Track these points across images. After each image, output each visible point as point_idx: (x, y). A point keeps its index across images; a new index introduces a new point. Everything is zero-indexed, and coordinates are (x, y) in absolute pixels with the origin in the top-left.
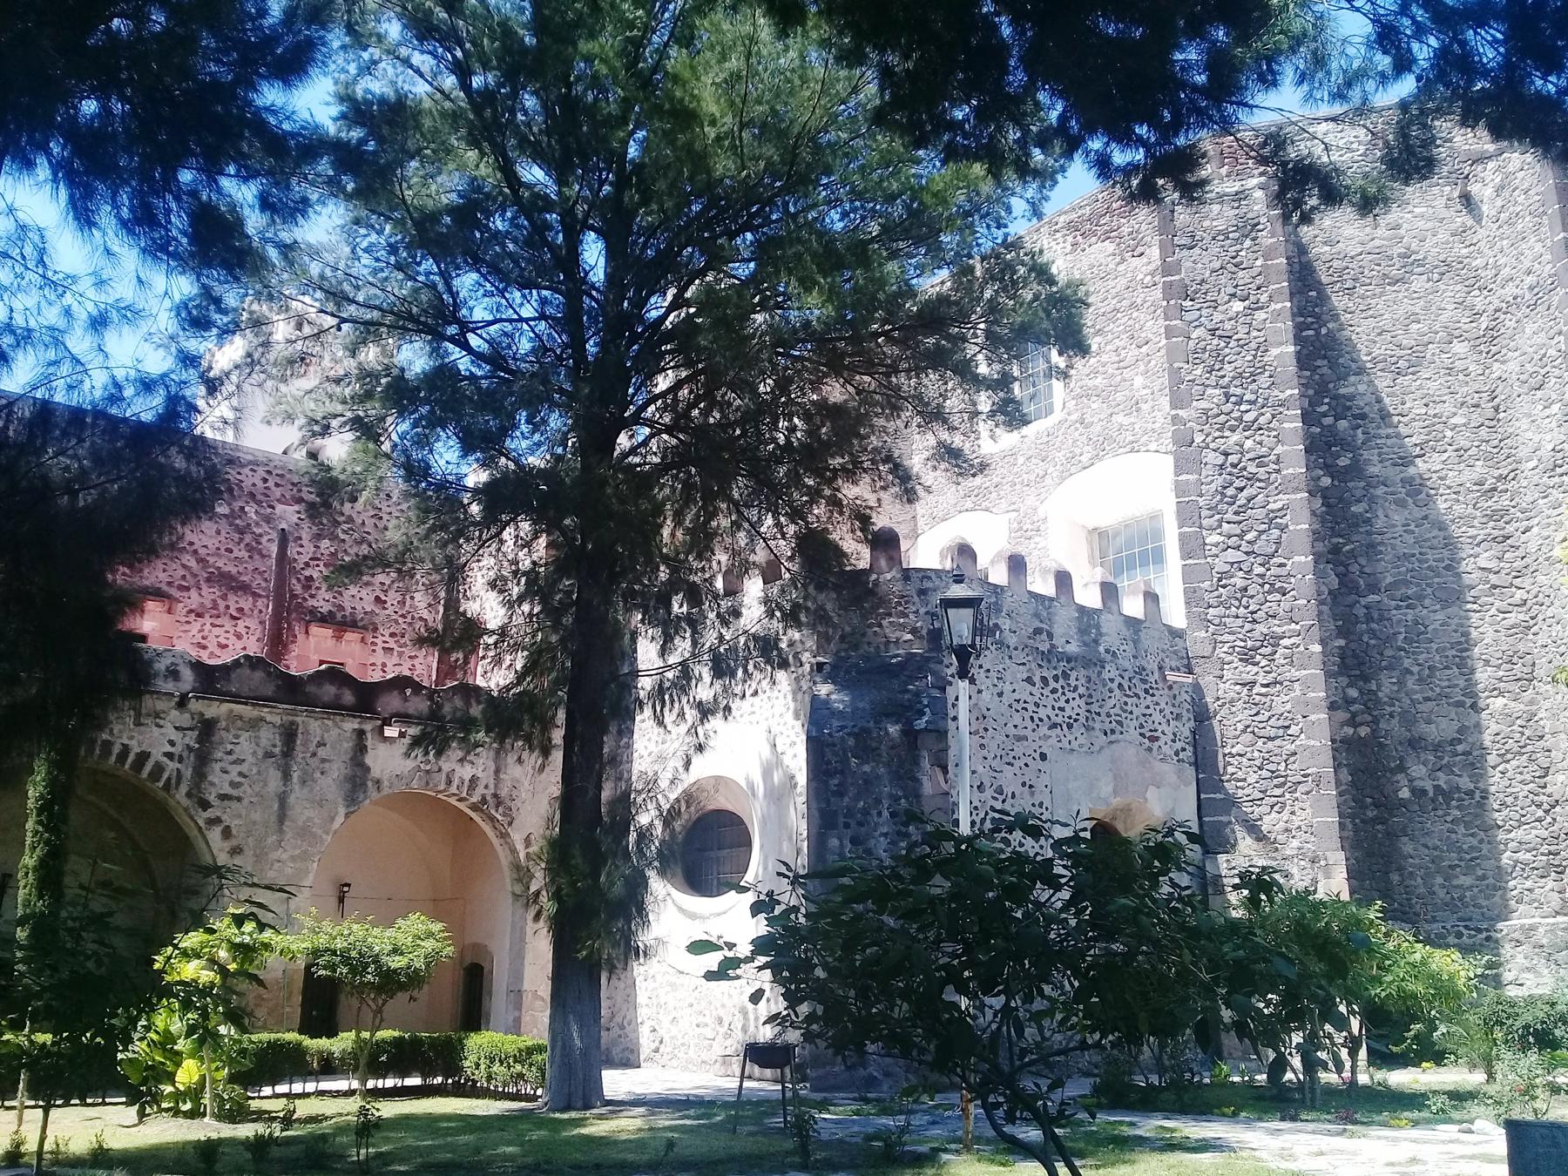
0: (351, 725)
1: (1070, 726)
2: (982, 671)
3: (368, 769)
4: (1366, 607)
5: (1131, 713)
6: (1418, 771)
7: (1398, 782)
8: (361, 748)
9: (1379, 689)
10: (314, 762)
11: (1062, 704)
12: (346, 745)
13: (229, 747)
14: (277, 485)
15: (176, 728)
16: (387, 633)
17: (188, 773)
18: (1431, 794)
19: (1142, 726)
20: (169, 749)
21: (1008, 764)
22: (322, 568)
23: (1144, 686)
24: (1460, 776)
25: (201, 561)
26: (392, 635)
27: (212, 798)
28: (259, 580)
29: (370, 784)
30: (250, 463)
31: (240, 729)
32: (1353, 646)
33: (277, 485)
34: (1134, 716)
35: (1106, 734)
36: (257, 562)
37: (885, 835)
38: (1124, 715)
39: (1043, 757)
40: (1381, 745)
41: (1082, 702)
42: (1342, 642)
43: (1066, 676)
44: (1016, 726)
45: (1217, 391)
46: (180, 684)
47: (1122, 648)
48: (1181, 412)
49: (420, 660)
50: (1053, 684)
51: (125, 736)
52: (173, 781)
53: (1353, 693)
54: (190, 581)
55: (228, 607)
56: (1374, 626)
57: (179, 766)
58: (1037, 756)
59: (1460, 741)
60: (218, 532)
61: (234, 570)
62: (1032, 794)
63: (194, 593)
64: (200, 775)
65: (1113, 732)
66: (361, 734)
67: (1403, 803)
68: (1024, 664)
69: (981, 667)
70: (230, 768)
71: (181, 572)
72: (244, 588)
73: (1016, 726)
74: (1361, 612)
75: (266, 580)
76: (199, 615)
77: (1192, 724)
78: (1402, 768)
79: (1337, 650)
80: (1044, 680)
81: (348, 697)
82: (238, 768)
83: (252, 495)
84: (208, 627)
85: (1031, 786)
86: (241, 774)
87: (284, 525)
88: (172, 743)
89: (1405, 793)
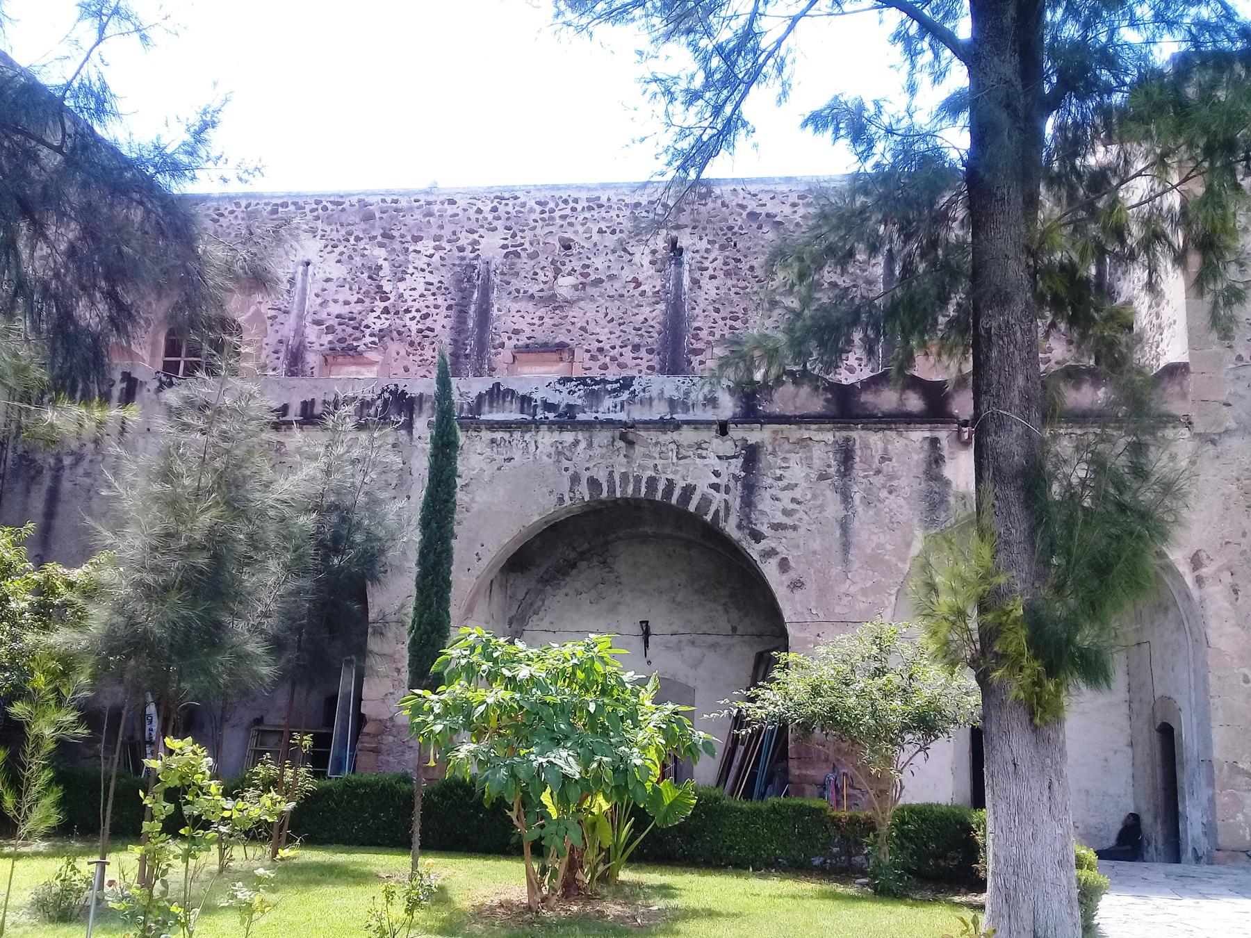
0: (918, 436)
3: (947, 483)
10: (878, 480)
12: (915, 457)
13: (778, 472)
15: (720, 458)
17: (736, 504)
20: (714, 480)
27: (764, 529)
29: (952, 500)
31: (787, 452)
46: (719, 412)
51: (669, 471)
52: (722, 514)
57: (726, 497)
64: (748, 503)
66: (934, 442)
70: (781, 495)
82: (789, 494)
86: (793, 500)
88: (717, 474)
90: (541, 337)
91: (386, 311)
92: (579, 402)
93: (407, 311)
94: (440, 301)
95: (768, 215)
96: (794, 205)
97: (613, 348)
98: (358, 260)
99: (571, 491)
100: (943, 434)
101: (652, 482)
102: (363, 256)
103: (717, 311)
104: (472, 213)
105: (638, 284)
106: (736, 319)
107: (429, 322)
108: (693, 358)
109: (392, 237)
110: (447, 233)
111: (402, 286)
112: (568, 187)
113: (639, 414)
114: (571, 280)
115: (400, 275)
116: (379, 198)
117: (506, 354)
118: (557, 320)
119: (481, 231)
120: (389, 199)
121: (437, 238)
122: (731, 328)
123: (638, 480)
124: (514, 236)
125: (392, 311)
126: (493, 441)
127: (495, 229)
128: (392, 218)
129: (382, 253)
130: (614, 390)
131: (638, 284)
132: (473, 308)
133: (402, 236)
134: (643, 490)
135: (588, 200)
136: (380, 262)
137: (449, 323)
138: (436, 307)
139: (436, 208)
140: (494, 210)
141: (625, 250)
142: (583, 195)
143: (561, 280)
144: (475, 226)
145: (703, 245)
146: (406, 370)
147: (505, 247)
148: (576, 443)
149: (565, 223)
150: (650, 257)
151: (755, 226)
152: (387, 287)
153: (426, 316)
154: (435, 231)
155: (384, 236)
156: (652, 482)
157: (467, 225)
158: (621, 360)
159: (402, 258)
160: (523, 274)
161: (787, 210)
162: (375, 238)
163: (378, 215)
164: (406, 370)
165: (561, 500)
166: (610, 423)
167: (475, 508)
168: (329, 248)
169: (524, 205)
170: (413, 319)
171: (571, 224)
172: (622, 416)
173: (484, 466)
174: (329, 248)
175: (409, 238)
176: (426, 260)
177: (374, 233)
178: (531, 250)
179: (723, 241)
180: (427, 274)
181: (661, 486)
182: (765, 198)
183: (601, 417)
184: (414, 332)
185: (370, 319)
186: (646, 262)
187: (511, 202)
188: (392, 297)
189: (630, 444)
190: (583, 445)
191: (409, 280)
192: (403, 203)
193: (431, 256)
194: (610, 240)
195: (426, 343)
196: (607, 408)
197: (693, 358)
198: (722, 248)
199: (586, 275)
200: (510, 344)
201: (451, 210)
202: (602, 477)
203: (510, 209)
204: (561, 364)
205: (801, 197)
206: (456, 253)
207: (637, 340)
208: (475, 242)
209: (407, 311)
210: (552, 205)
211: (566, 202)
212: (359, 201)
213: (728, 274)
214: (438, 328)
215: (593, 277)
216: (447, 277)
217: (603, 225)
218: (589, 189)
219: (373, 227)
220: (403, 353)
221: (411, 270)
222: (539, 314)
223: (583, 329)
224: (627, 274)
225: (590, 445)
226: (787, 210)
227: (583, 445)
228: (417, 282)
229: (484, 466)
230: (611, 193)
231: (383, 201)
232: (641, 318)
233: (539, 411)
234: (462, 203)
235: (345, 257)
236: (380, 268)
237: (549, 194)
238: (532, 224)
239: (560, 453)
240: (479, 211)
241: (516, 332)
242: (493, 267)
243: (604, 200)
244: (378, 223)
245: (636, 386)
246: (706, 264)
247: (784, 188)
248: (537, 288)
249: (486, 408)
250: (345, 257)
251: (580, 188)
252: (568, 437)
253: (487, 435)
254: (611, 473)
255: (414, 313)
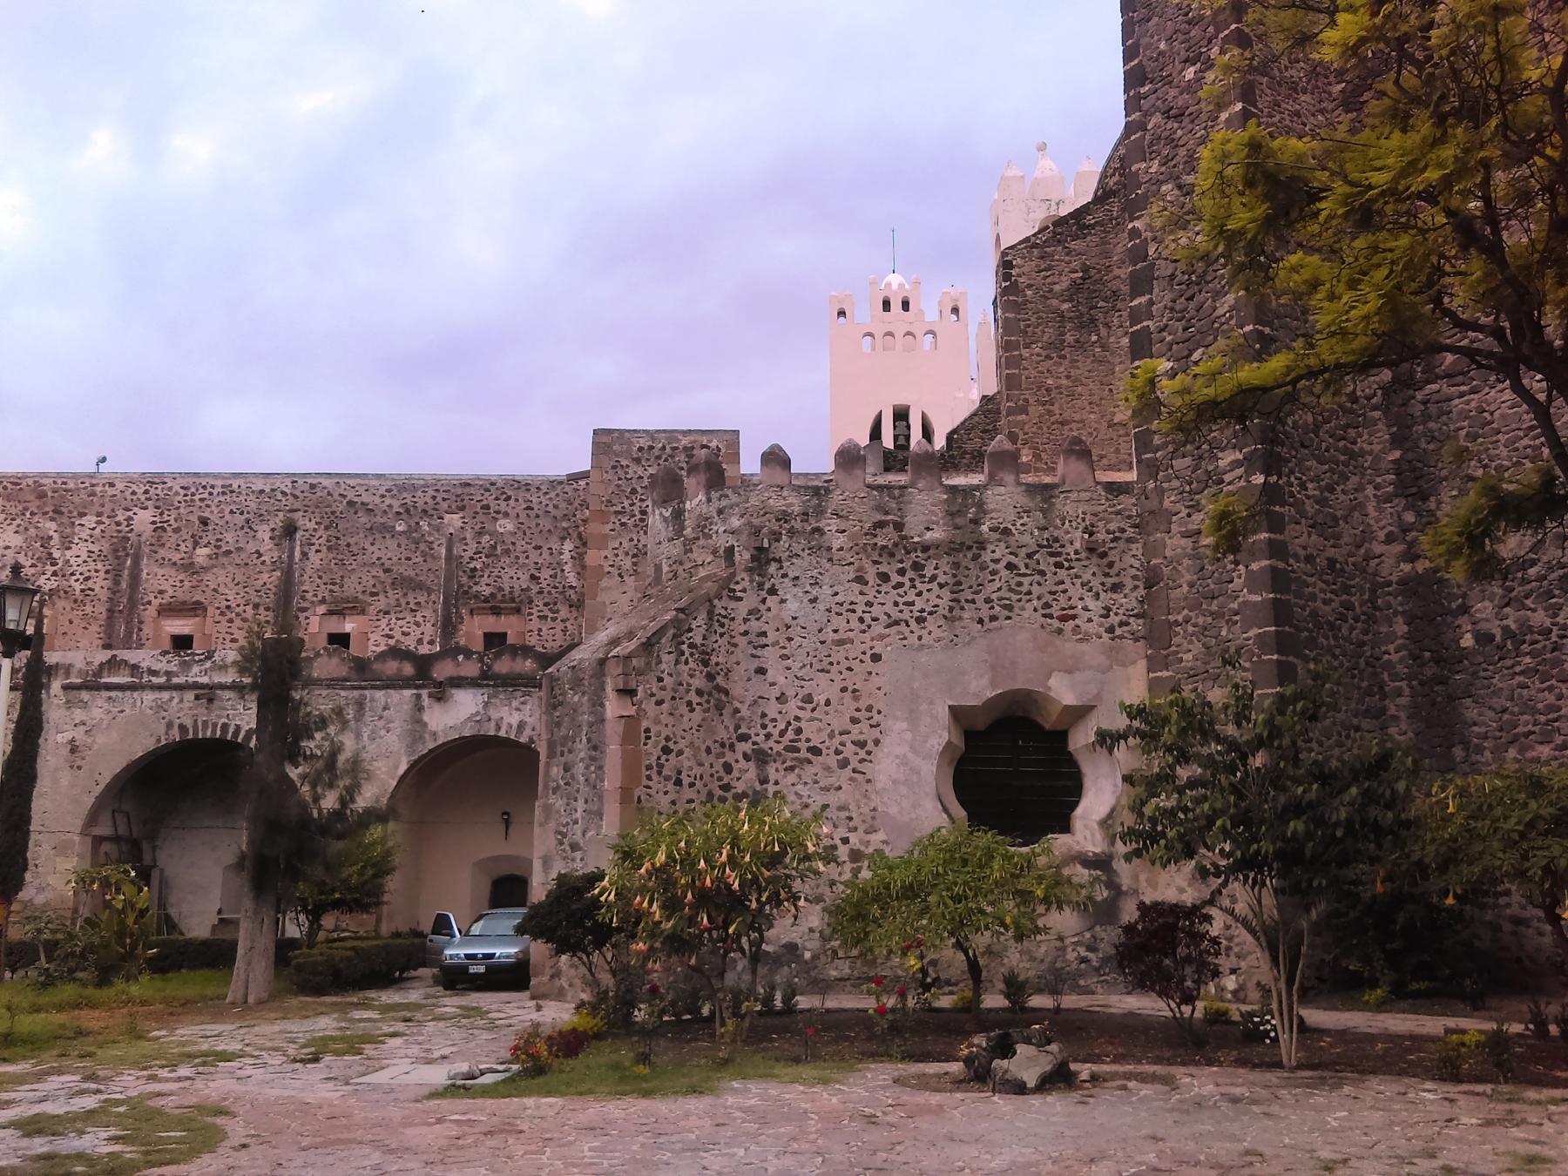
0: (408, 693)
1: (920, 620)
2: (786, 580)
3: (425, 725)
4: (1425, 403)
5: (1029, 593)
6: (1484, 609)
7: (1459, 627)
8: (419, 708)
9: (1438, 508)
10: (381, 723)
11: (911, 597)
14: (444, 499)
16: (541, 603)
18: (1498, 639)
19: (1047, 605)
21: (822, 671)
22: (484, 559)
23: (1053, 560)
24: (1534, 610)
25: (387, 571)
26: (546, 604)
28: (432, 577)
29: (427, 736)
30: (423, 486)
32: (1410, 456)
33: (444, 499)
34: (1035, 595)
35: (981, 621)
36: (431, 564)
37: (582, 760)
38: (1015, 597)
39: (876, 658)
40: (1441, 581)
41: (946, 593)
42: (1397, 454)
43: (917, 567)
44: (836, 631)
45: (1170, 186)
47: (1019, 522)
48: (1137, 224)
49: (572, 621)
50: (895, 578)
53: (1410, 517)
54: (379, 587)
55: (408, 603)
56: (1432, 425)
58: (867, 658)
59: (1533, 563)
60: (399, 546)
61: (412, 574)
62: (856, 699)
63: (381, 597)
65: (993, 618)
66: (419, 697)
67: (1464, 654)
68: (852, 563)
69: (785, 576)
71: (372, 582)
72: (420, 586)
73: (836, 631)
74: (1417, 409)
75: (438, 577)
76: (387, 613)
77: (1142, 592)
78: (1465, 610)
79: (1391, 466)
80: (885, 578)
81: (408, 669)
83: (425, 511)
84: (394, 620)
85: (854, 691)
87: (452, 531)
89: (1467, 641)
90: (181, 596)
91: (55, 574)
92: (175, 669)
93: (72, 574)
94: (99, 566)
95: (363, 504)
96: (383, 496)
97: (238, 606)
98: (32, 531)
99: (167, 734)
100: (424, 693)
101: (225, 727)
102: (37, 528)
103: (320, 577)
104: (128, 494)
105: (260, 555)
106: (334, 584)
107: (90, 584)
108: (300, 614)
109: (62, 513)
110: (107, 510)
111: (68, 553)
112: (207, 475)
113: (219, 678)
114: (206, 551)
115: (67, 544)
116: (51, 480)
117: (151, 611)
118: (195, 583)
119: (135, 510)
120: (59, 481)
121: (99, 514)
122: (331, 591)
123: (215, 725)
124: (162, 514)
125: (60, 574)
126: (110, 698)
127: (146, 508)
128: (62, 497)
129: (53, 526)
130: (201, 660)
131: (260, 555)
132: (126, 572)
133: (70, 512)
134: (218, 732)
135: (223, 486)
136: (51, 533)
137: (107, 584)
138: (96, 571)
139: (98, 489)
140: (146, 492)
141: (250, 528)
142: (219, 483)
143: (199, 551)
144: (129, 504)
145: (312, 525)
146: (71, 622)
147: (154, 523)
148: (172, 698)
149: (203, 505)
150: (270, 534)
151: (352, 511)
152: (56, 554)
153: (87, 579)
154: (97, 508)
155: (55, 511)
156: (225, 727)
157: (124, 504)
158: (244, 615)
159: (68, 530)
160: (168, 545)
161: (377, 500)
162: (47, 513)
163: (50, 494)
164: (71, 622)
165: (159, 741)
166: (195, 686)
167: (96, 747)
168: (8, 521)
169: (170, 489)
170: (77, 580)
171: (208, 506)
172: (205, 680)
173: (103, 717)
174: (8, 521)
175: (75, 514)
176: (89, 532)
177: (47, 509)
178: (175, 526)
179: (327, 522)
180: (89, 544)
181: (231, 730)
182: (361, 490)
183: (190, 680)
184: (78, 592)
185: (42, 581)
186: (267, 537)
187: (160, 487)
188: (60, 563)
189: (211, 701)
190: (176, 700)
191: (75, 550)
192: (71, 485)
193: (93, 529)
194: (240, 519)
195: (87, 600)
196: (196, 675)
197: (300, 614)
198: (327, 528)
199: (218, 547)
200: (156, 602)
201: (111, 491)
202: (188, 722)
203: (159, 492)
204: (197, 619)
205: (387, 491)
206: (114, 527)
207: (257, 600)
208: (129, 519)
209: (72, 574)
210: (193, 490)
211: (204, 487)
212: (35, 482)
213: (329, 548)
214: (97, 589)
215: (224, 549)
216: (106, 546)
217: (234, 508)
218: (224, 478)
219: (45, 503)
220: (68, 608)
221: (76, 541)
222: (180, 578)
223: (215, 590)
224: (252, 547)
225: (181, 701)
226: (377, 500)
227: (176, 700)
228: (80, 550)
229: (103, 717)
230: (241, 482)
231: (55, 482)
232: (261, 582)
233: (145, 675)
234: (120, 486)
235: (21, 529)
236: (51, 538)
237: (191, 480)
238: (176, 504)
239: (161, 707)
240: (134, 493)
241: (161, 592)
242: (143, 539)
243: (235, 486)
244: (50, 501)
245: (216, 657)
246: (314, 540)
247: (375, 483)
248: (179, 556)
249: (106, 674)
250: (21, 529)
251: (216, 476)
252: (166, 695)
253: (105, 694)
254: (196, 721)
255: (78, 576)
